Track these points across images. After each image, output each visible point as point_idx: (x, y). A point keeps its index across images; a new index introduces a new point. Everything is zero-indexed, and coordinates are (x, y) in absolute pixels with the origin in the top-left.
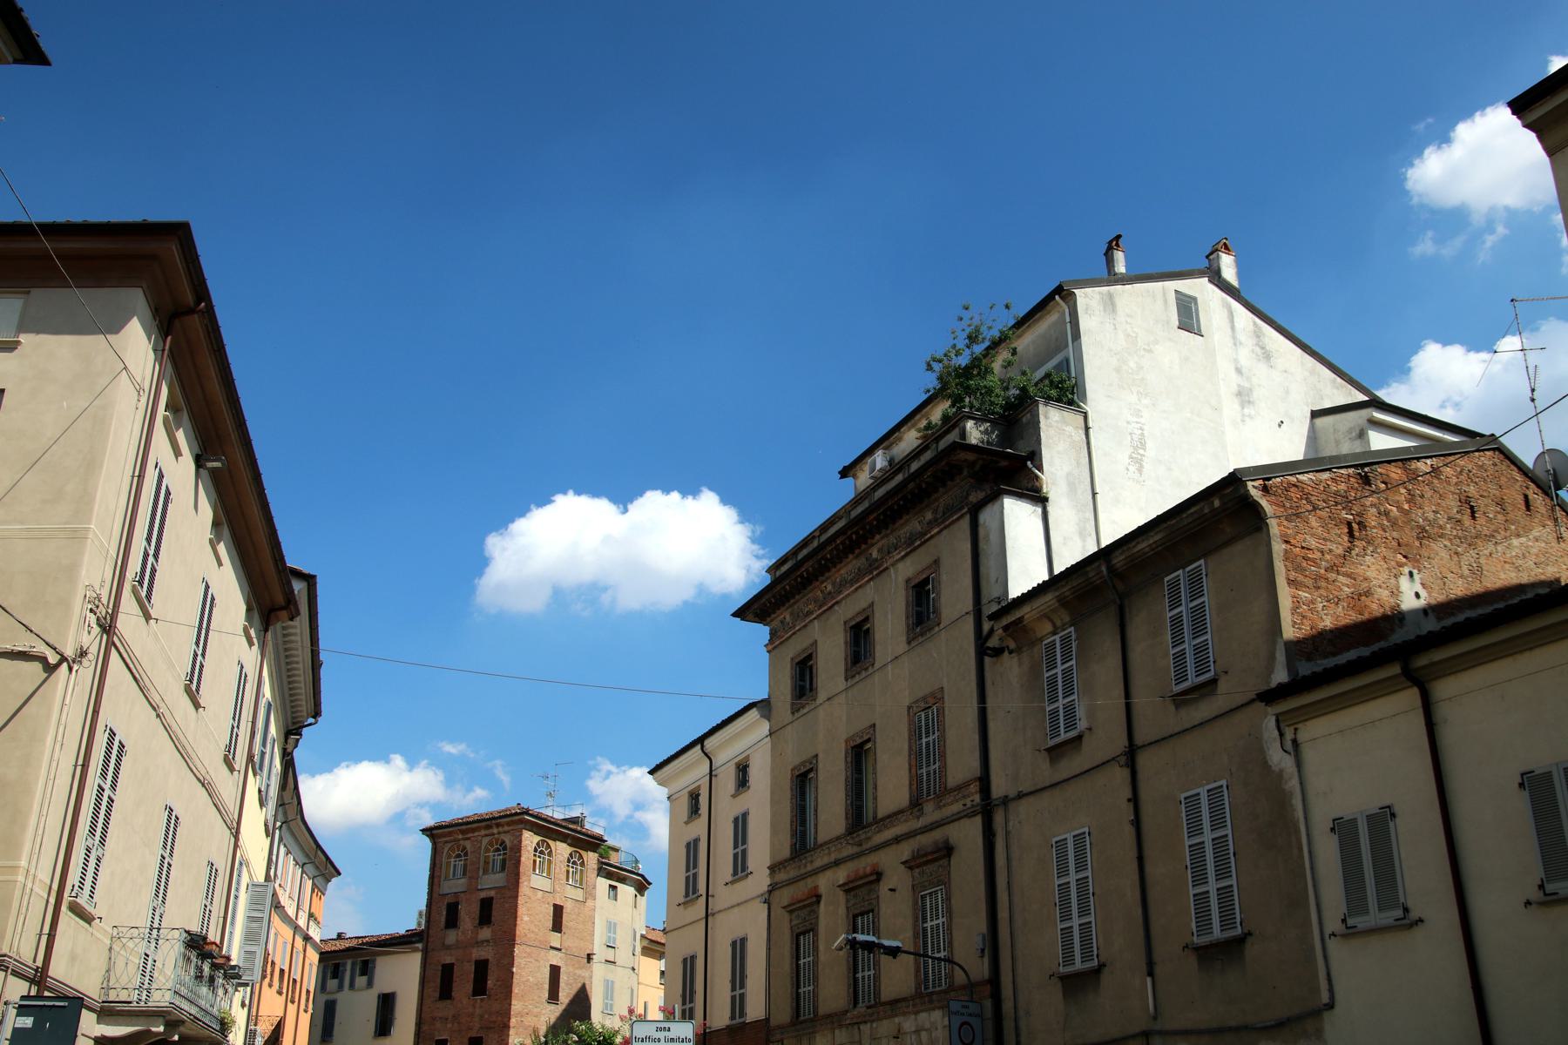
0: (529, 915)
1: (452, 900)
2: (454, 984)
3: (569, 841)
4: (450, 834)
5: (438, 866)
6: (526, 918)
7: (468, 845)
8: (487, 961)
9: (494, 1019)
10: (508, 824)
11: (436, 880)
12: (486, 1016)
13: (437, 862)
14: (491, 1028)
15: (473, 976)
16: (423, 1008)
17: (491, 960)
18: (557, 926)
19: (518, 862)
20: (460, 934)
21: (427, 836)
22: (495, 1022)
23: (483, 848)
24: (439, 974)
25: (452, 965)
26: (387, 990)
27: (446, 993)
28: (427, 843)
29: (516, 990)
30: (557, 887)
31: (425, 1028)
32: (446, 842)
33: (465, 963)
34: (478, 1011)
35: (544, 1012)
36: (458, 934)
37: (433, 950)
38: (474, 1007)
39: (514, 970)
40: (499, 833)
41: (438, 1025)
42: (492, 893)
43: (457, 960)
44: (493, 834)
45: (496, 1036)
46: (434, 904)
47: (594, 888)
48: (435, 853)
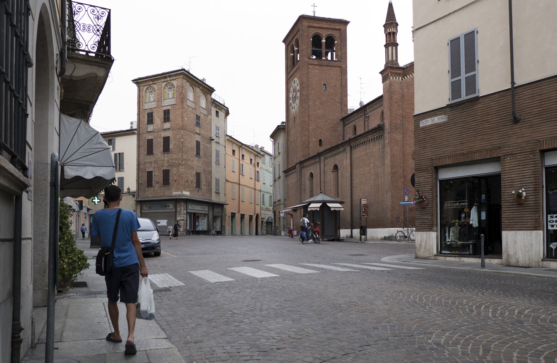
0: (187, 118)
1: (150, 111)
2: (154, 148)
3: (201, 88)
5: (141, 97)
8: (169, 137)
9: (174, 161)
10: (175, 75)
12: (170, 161)
13: (141, 95)
15: (162, 144)
17: (171, 137)
18: (198, 124)
20: (155, 126)
21: (135, 83)
22: (175, 163)
24: (146, 143)
25: (152, 140)
27: (150, 151)
28: (135, 87)
30: (197, 107)
31: (141, 166)
32: (144, 86)
33: (158, 139)
34: (166, 158)
35: (195, 160)
36: (154, 126)
37: (142, 133)
40: (171, 80)
41: (148, 165)
42: (169, 108)
43: (154, 137)
45: (176, 169)
46: (141, 113)
47: (211, 110)
48: (139, 91)
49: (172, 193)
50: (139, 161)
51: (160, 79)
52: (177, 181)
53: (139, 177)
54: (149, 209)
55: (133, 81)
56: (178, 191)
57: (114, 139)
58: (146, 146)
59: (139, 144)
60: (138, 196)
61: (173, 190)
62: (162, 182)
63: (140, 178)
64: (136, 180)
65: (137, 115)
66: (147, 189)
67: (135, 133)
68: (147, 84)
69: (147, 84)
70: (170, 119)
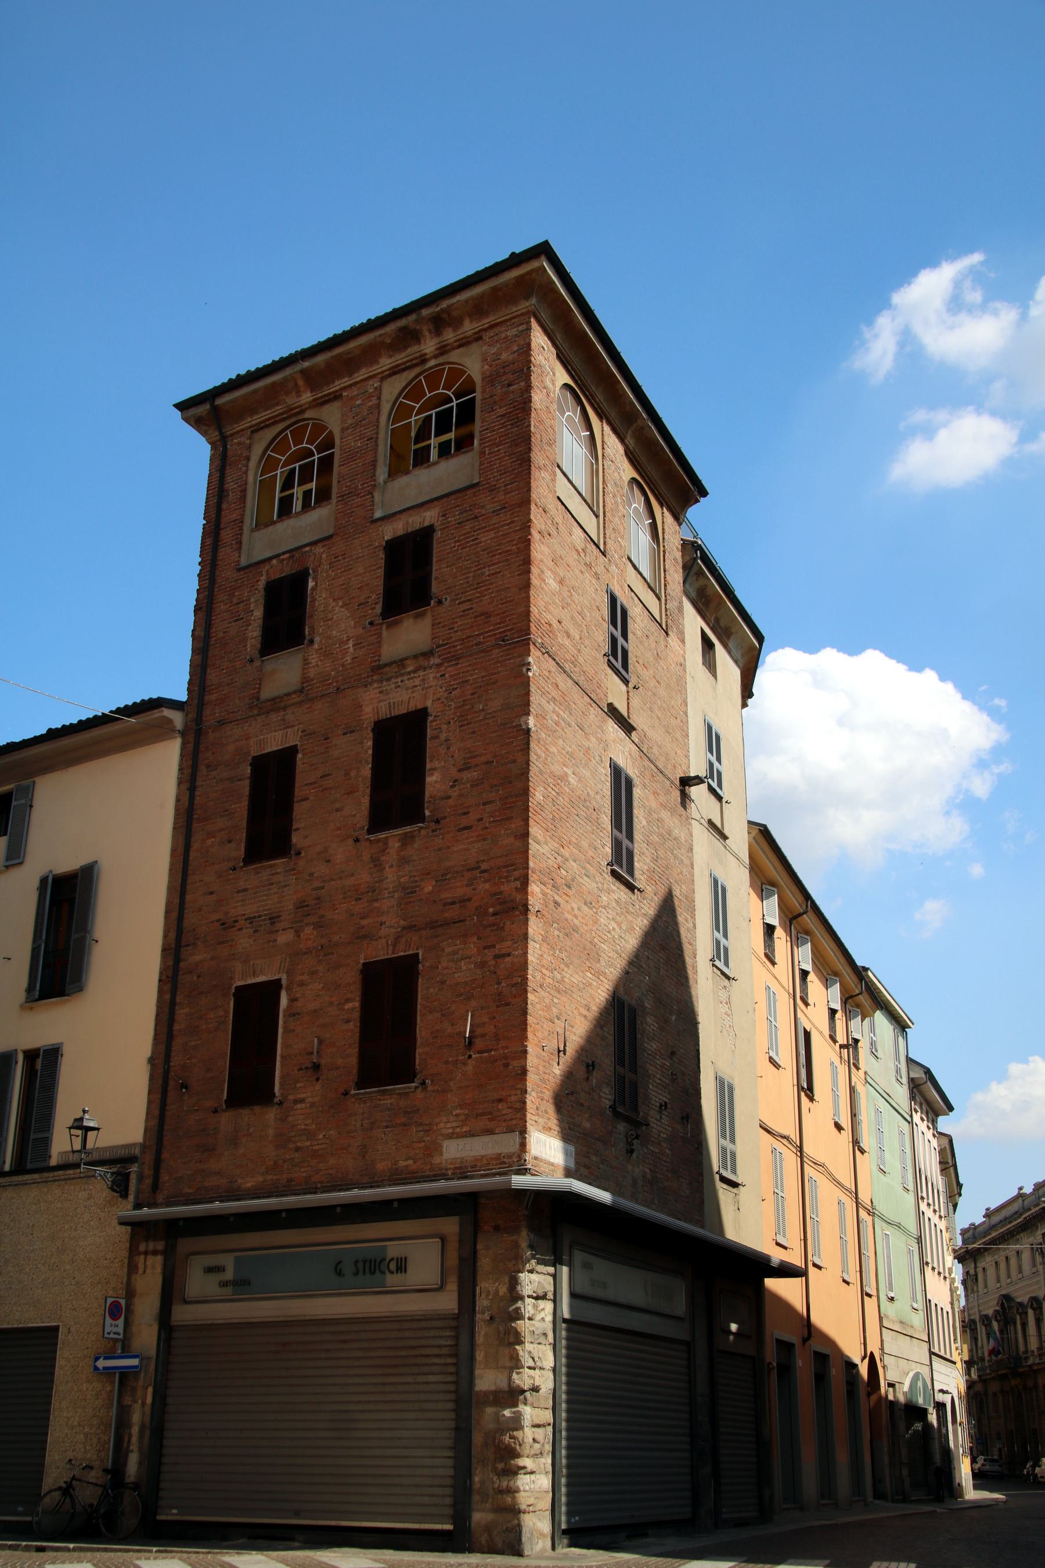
2: (300, 810)
3: (630, 441)
4: (273, 394)
5: (231, 497)
6: (552, 583)
7: (332, 417)
9: (459, 889)
10: (478, 309)
11: (226, 535)
13: (230, 485)
14: (447, 923)
15: (367, 771)
16: (189, 897)
19: (523, 407)
20: (314, 659)
22: (464, 901)
23: (386, 408)
24: (245, 787)
26: (67, 863)
29: (538, 795)
31: (196, 956)
32: (257, 429)
34: (391, 875)
36: (306, 662)
37: (222, 723)
38: (377, 863)
39: (532, 722)
41: (244, 942)
42: (429, 517)
43: (306, 734)
44: (423, 360)
45: (472, 948)
49: (434, 1149)
50: (181, 918)
51: (370, 354)
52: (479, 1043)
53: (170, 1037)
54: (229, 1290)
55: (181, 406)
56: (490, 1132)
57: (28, 792)
58: (245, 803)
59: (192, 797)
60: (155, 1187)
61: (445, 1124)
62: (353, 1061)
63: (178, 1043)
64: (151, 1060)
65: (197, 610)
66: (226, 1121)
67: (170, 721)
68: (279, 409)
69: (279, 409)
70: (435, 588)
